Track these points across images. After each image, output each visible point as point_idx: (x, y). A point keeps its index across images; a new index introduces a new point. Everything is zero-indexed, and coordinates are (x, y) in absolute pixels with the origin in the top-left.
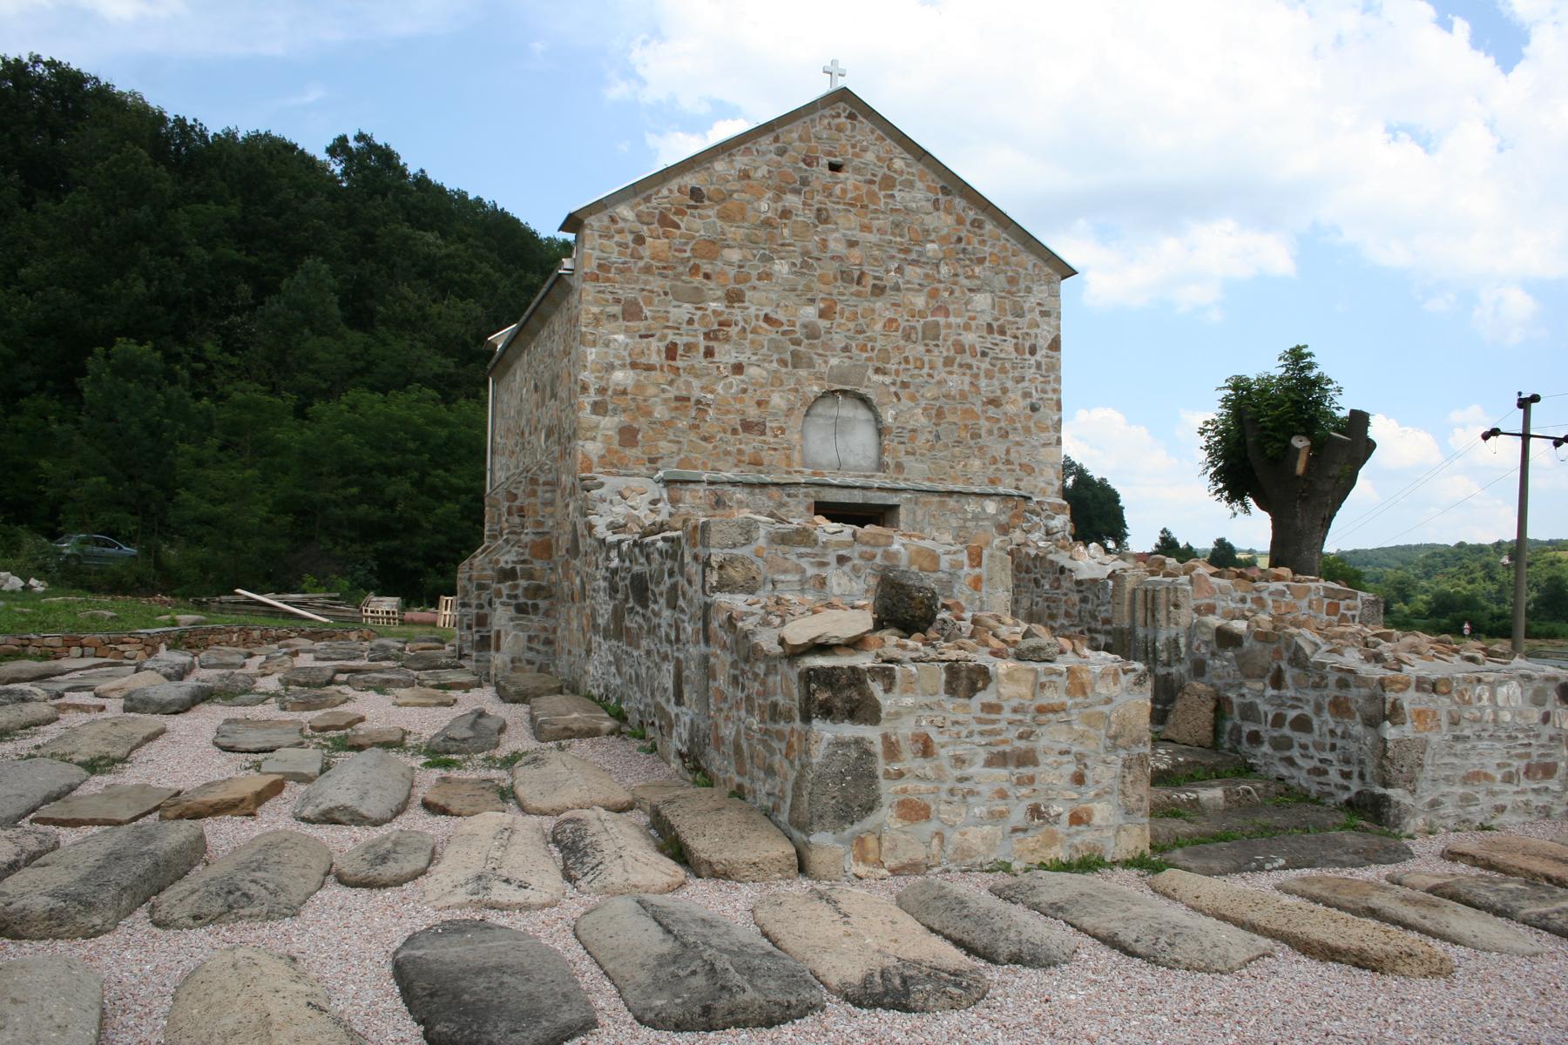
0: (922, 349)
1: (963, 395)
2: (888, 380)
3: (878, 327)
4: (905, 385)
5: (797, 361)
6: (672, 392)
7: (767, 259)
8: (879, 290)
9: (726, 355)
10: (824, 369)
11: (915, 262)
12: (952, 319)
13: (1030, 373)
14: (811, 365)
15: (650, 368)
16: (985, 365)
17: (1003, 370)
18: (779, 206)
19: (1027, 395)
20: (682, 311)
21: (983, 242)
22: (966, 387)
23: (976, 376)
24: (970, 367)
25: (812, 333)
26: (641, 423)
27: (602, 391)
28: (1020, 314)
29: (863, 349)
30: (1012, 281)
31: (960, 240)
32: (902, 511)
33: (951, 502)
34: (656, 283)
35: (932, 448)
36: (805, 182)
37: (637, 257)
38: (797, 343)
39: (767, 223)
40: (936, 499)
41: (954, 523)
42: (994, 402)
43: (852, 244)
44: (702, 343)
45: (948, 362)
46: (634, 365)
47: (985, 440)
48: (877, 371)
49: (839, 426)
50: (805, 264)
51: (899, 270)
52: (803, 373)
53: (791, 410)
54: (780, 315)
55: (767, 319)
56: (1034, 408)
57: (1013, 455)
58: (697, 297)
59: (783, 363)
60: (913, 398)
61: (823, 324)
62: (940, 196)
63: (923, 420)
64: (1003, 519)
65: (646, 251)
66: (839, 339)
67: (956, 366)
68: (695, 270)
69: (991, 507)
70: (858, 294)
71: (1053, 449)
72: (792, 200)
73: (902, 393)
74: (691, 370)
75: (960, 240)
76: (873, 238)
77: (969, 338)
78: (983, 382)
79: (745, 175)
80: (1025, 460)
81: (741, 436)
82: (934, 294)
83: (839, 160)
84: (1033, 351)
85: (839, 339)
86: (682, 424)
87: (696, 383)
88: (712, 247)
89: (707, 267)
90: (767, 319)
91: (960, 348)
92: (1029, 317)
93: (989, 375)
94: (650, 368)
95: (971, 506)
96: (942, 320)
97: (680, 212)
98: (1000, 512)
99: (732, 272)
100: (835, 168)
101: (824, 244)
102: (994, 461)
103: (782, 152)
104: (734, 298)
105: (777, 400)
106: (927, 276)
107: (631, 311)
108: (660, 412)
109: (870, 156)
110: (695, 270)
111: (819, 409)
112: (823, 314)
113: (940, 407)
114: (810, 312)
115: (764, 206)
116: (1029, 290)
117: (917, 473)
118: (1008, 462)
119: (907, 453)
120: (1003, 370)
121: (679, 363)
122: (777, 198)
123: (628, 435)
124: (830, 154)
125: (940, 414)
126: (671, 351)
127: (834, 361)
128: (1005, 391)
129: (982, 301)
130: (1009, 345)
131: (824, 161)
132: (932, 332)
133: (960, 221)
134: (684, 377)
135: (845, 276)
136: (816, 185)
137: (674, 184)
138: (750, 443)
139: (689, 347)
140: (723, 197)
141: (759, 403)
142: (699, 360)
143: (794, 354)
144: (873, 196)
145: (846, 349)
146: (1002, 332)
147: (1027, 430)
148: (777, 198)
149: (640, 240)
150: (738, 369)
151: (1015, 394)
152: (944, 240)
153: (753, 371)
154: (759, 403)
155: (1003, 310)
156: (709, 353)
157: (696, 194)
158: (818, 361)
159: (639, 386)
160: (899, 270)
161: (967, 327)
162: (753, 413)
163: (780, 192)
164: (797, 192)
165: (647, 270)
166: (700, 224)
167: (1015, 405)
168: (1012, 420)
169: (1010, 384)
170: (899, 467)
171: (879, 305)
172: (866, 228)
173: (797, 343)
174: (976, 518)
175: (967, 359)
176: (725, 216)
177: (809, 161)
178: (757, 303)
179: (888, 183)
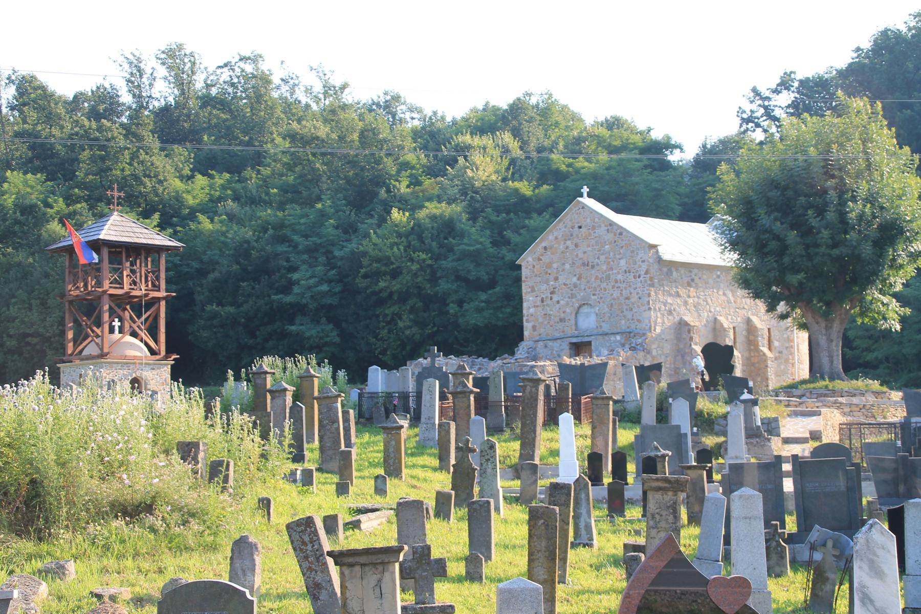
0: (605, 284)
1: (618, 298)
2: (595, 297)
3: (593, 279)
4: (601, 298)
5: (573, 296)
6: (543, 313)
7: (564, 264)
8: (593, 267)
9: (555, 298)
10: (579, 297)
11: (603, 254)
12: (614, 271)
13: (639, 285)
14: (576, 297)
15: (537, 306)
16: (624, 285)
17: (630, 286)
18: (565, 246)
19: (638, 293)
20: (544, 287)
21: (622, 240)
22: (619, 295)
23: (622, 290)
24: (619, 287)
25: (575, 286)
26: (537, 324)
27: (527, 316)
28: (635, 263)
29: (589, 288)
30: (632, 252)
31: (615, 242)
32: (593, 343)
33: (606, 338)
34: (538, 279)
35: (610, 318)
36: (572, 235)
37: (533, 272)
38: (572, 290)
39: (562, 252)
40: (600, 337)
41: (608, 345)
42: (628, 298)
43: (585, 253)
44: (550, 296)
45: (613, 287)
46: (535, 306)
47: (626, 313)
48: (594, 295)
49: (587, 315)
50: (573, 263)
51: (598, 258)
52: (574, 300)
53: (572, 313)
54: (568, 282)
55: (565, 284)
56: (640, 298)
57: (635, 317)
58: (547, 282)
59: (569, 298)
60: (603, 302)
61: (578, 282)
62: (609, 227)
63: (607, 309)
64: (623, 341)
65: (535, 270)
66: (583, 287)
67: (615, 289)
68: (546, 273)
69: (618, 338)
70: (587, 270)
71: (647, 312)
72: (569, 243)
73: (601, 301)
74: (547, 305)
75: (615, 242)
76: (590, 249)
77: (619, 277)
78: (624, 292)
79: (556, 238)
80: (639, 318)
81: (560, 324)
82: (608, 263)
83: (579, 225)
84: (639, 277)
85: (583, 287)
86: (546, 322)
87: (548, 309)
88: (549, 265)
89: (549, 272)
90: (565, 284)
91: (616, 281)
92: (638, 263)
93: (626, 288)
94: (537, 306)
95: (612, 338)
96: (611, 272)
97: (542, 255)
98: (621, 339)
99: (555, 271)
100: (580, 227)
101: (577, 255)
102: (628, 320)
103: (565, 227)
104: (556, 279)
105: (568, 310)
106: (606, 258)
107: (533, 290)
108: (540, 320)
109: (588, 220)
110: (546, 273)
111: (581, 310)
112: (578, 279)
113: (612, 304)
114: (575, 279)
115: (561, 247)
116: (637, 254)
117: (606, 328)
118: (633, 320)
119: (603, 321)
120: (630, 286)
121: (545, 303)
122: (565, 243)
123: (534, 328)
124: (578, 223)
125: (612, 305)
126: (542, 301)
127: (582, 294)
128: (631, 293)
129: (623, 262)
130: (631, 277)
131: (577, 226)
132: (608, 278)
133: (615, 235)
134: (546, 307)
135: (584, 264)
136: (575, 235)
137: (540, 247)
138: (560, 326)
139: (547, 297)
140: (551, 247)
141: (564, 312)
142: (549, 302)
143: (572, 294)
144: (590, 235)
145: (585, 289)
146: (629, 272)
147: (638, 307)
148: (565, 243)
149: (534, 267)
150: (558, 302)
151: (634, 294)
152: (610, 243)
153: (562, 302)
154: (564, 312)
155: (630, 265)
156: (551, 299)
157: (545, 248)
158: (578, 295)
159: (536, 312)
160: (598, 258)
161: (618, 273)
162: (562, 315)
163: (566, 240)
164: (569, 239)
165: (536, 276)
166: (545, 259)
167: (634, 299)
168: (633, 304)
169: (632, 291)
170: (601, 327)
171: (593, 272)
172: (588, 246)
173: (572, 290)
174: (614, 342)
175: (619, 285)
176: (552, 254)
177: (573, 227)
178: (561, 280)
179: (594, 228)
